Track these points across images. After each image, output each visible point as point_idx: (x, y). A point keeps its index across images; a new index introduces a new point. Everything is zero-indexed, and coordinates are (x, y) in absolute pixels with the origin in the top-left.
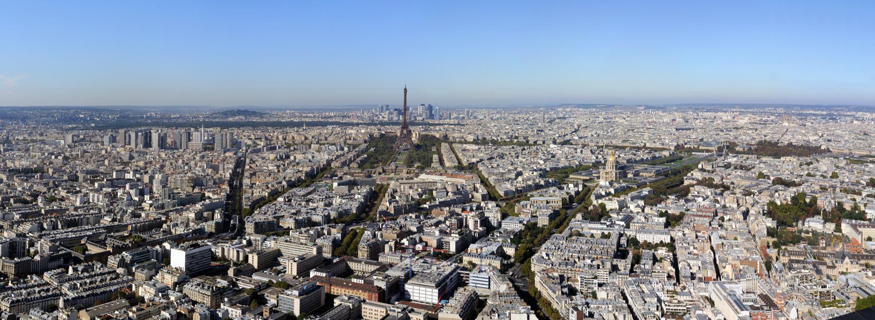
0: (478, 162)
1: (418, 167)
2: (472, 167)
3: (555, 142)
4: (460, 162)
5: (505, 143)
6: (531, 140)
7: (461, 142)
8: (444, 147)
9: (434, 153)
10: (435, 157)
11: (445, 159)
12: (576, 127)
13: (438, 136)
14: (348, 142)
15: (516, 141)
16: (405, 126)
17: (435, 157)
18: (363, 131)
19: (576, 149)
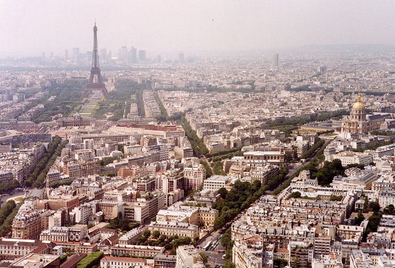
0: (186, 111)
1: (110, 119)
2: (179, 117)
3: (288, 88)
4: (163, 111)
5: (224, 90)
6: (259, 84)
7: (169, 90)
8: (146, 94)
9: (133, 101)
10: (134, 108)
11: (146, 107)
12: (319, 70)
13: (139, 82)
15: (238, 87)
16: (95, 70)
17: (134, 108)
19: (315, 96)
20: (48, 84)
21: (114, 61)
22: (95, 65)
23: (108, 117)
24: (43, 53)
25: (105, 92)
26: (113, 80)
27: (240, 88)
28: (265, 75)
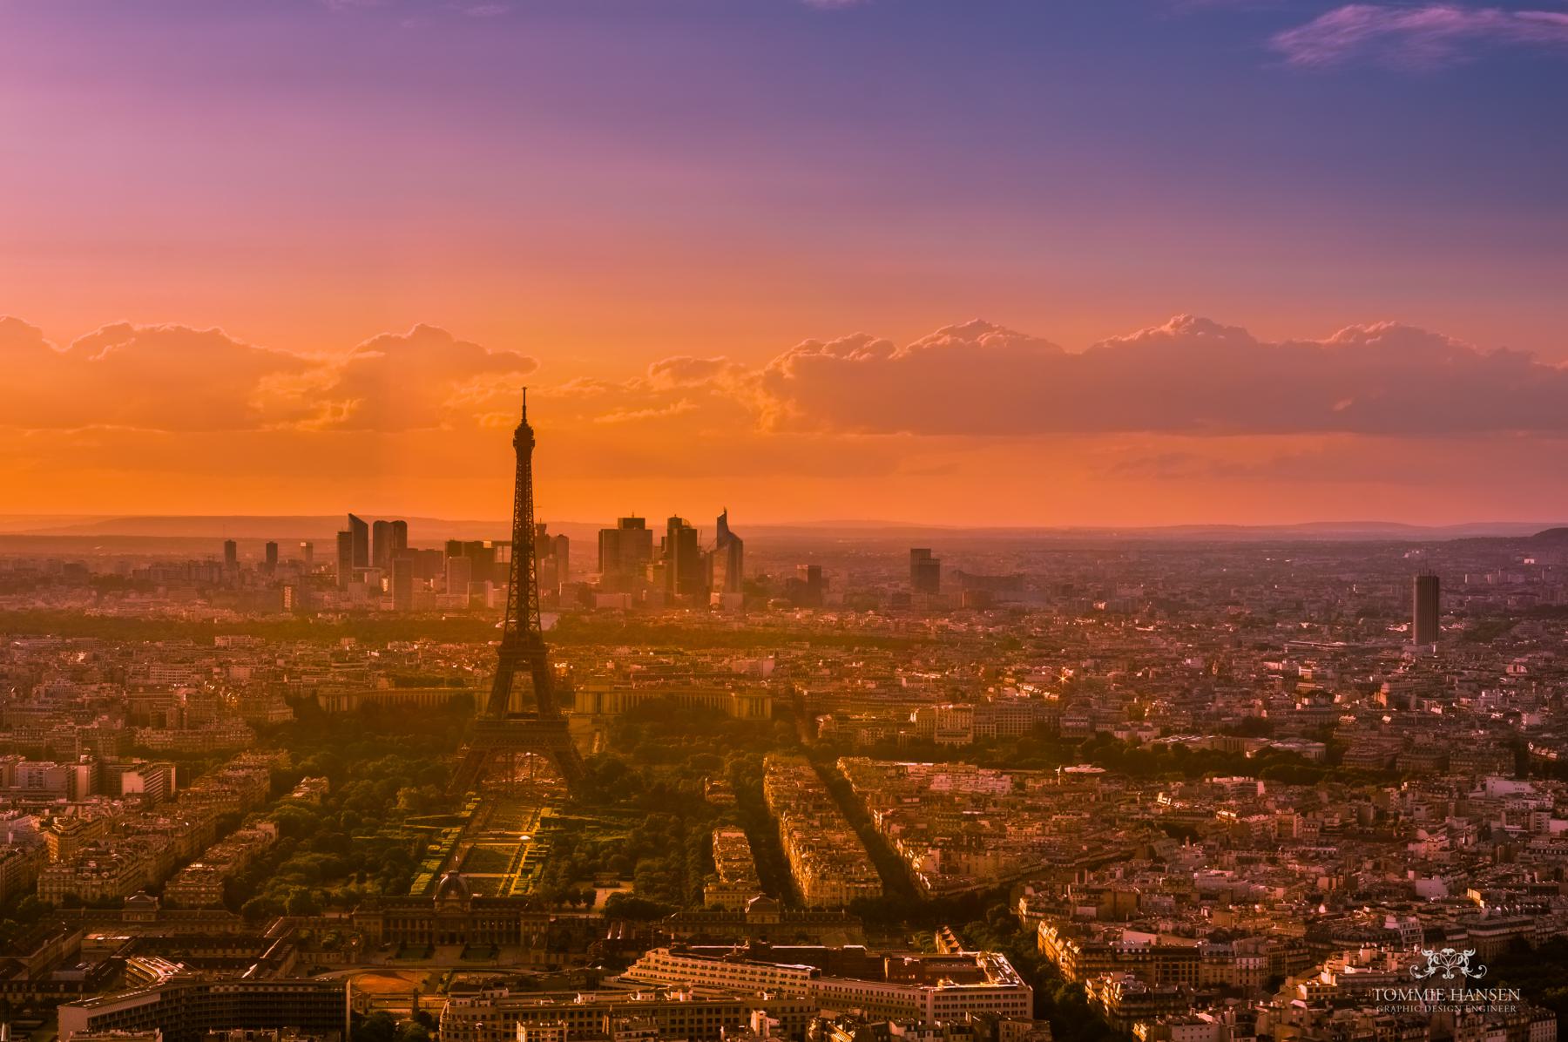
1: (620, 910)
4: (893, 870)
7: (890, 749)
10: (728, 841)
11: (795, 856)
13: (739, 706)
14: (150, 737)
16: (522, 648)
17: (728, 841)
18: (241, 673)
20: (280, 713)
21: (585, 594)
22: (523, 623)
23: (602, 896)
24: (230, 546)
25: (565, 761)
26: (599, 696)
27: (1261, 753)
28: (1385, 688)
